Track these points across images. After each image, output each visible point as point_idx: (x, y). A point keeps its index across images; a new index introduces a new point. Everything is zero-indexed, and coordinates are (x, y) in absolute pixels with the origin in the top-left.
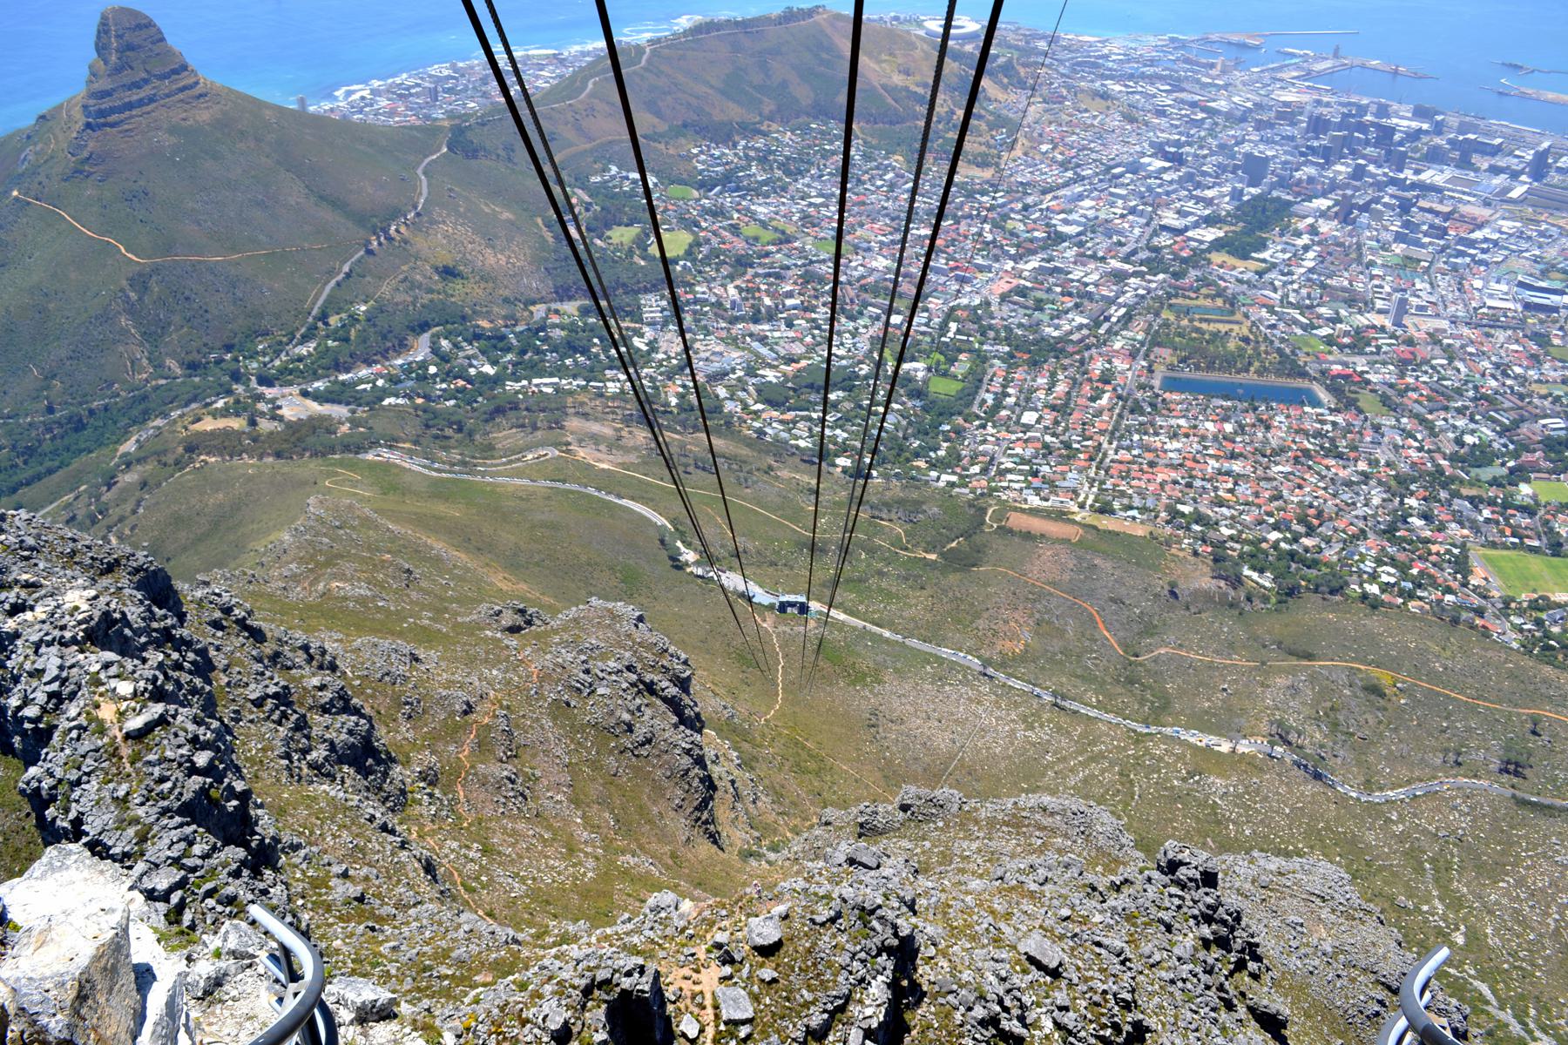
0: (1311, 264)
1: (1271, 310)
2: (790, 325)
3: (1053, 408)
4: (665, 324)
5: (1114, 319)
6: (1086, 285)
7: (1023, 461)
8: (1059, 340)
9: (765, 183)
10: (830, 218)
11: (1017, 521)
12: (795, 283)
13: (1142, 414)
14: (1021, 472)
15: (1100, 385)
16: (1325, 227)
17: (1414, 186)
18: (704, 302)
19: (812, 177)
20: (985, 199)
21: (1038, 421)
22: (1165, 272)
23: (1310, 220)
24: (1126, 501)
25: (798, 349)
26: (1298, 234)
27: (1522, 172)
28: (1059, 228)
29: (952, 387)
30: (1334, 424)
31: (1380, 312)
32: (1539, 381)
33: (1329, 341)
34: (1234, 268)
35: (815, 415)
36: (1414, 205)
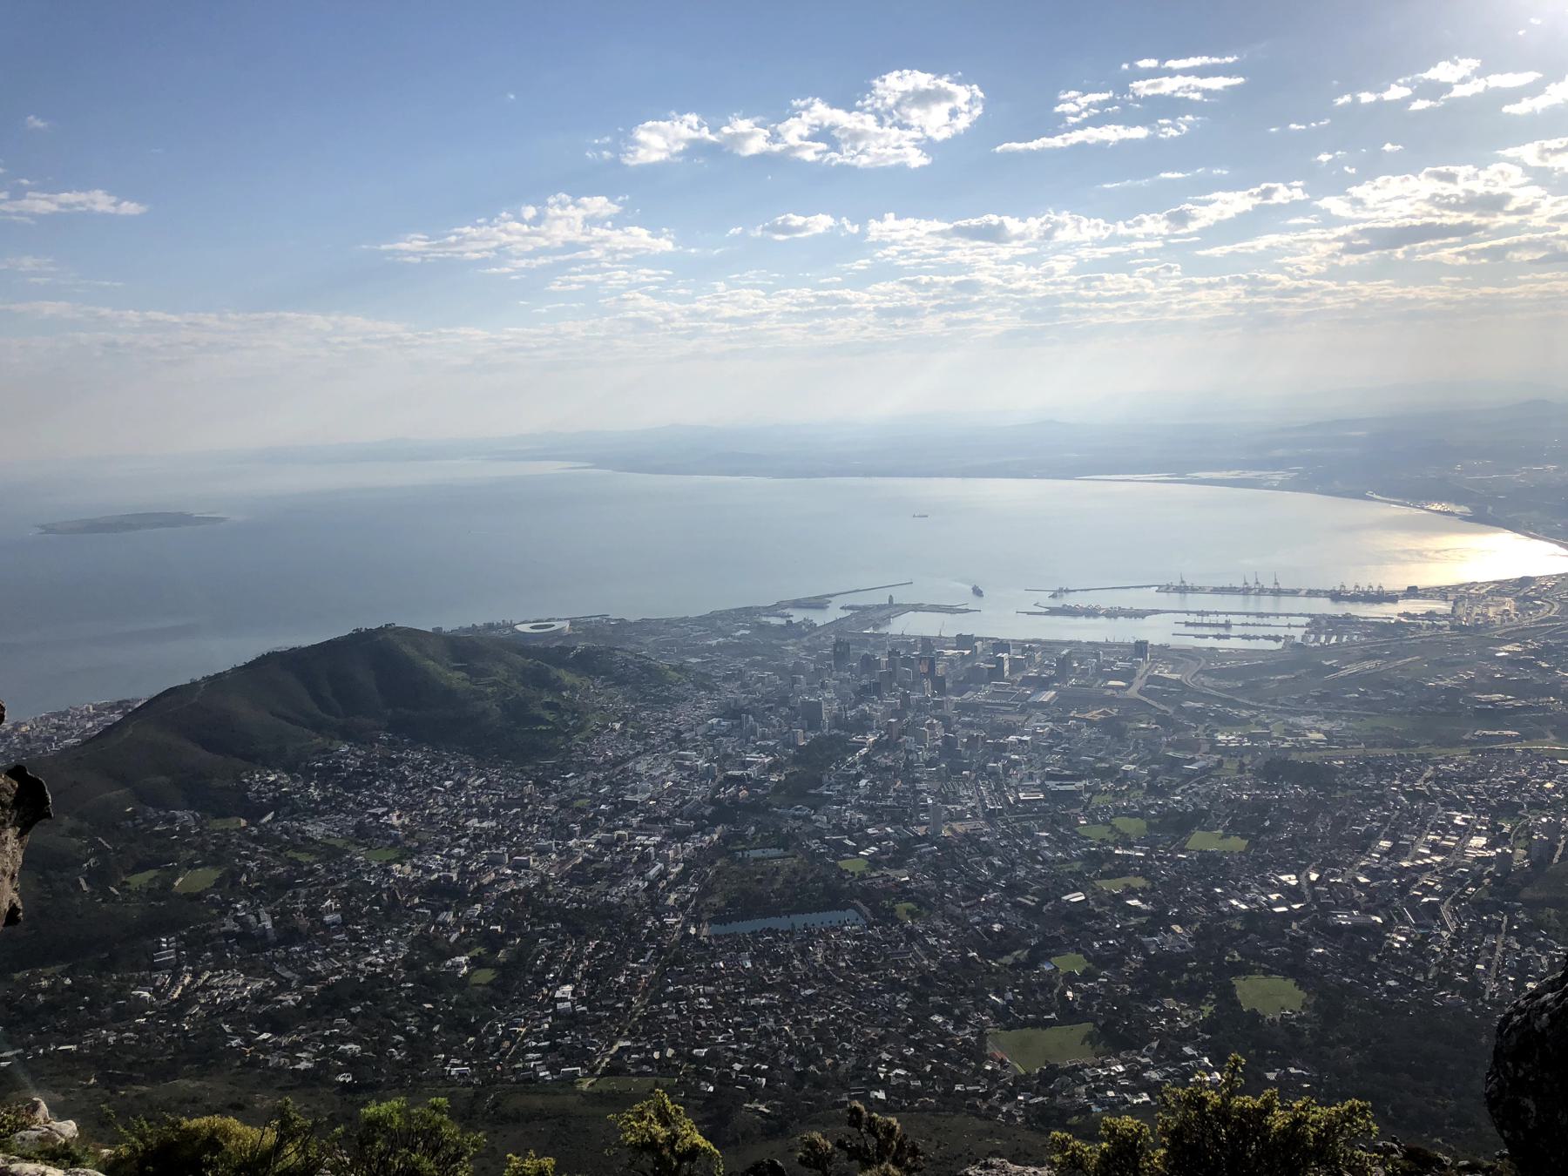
18: (228, 935)
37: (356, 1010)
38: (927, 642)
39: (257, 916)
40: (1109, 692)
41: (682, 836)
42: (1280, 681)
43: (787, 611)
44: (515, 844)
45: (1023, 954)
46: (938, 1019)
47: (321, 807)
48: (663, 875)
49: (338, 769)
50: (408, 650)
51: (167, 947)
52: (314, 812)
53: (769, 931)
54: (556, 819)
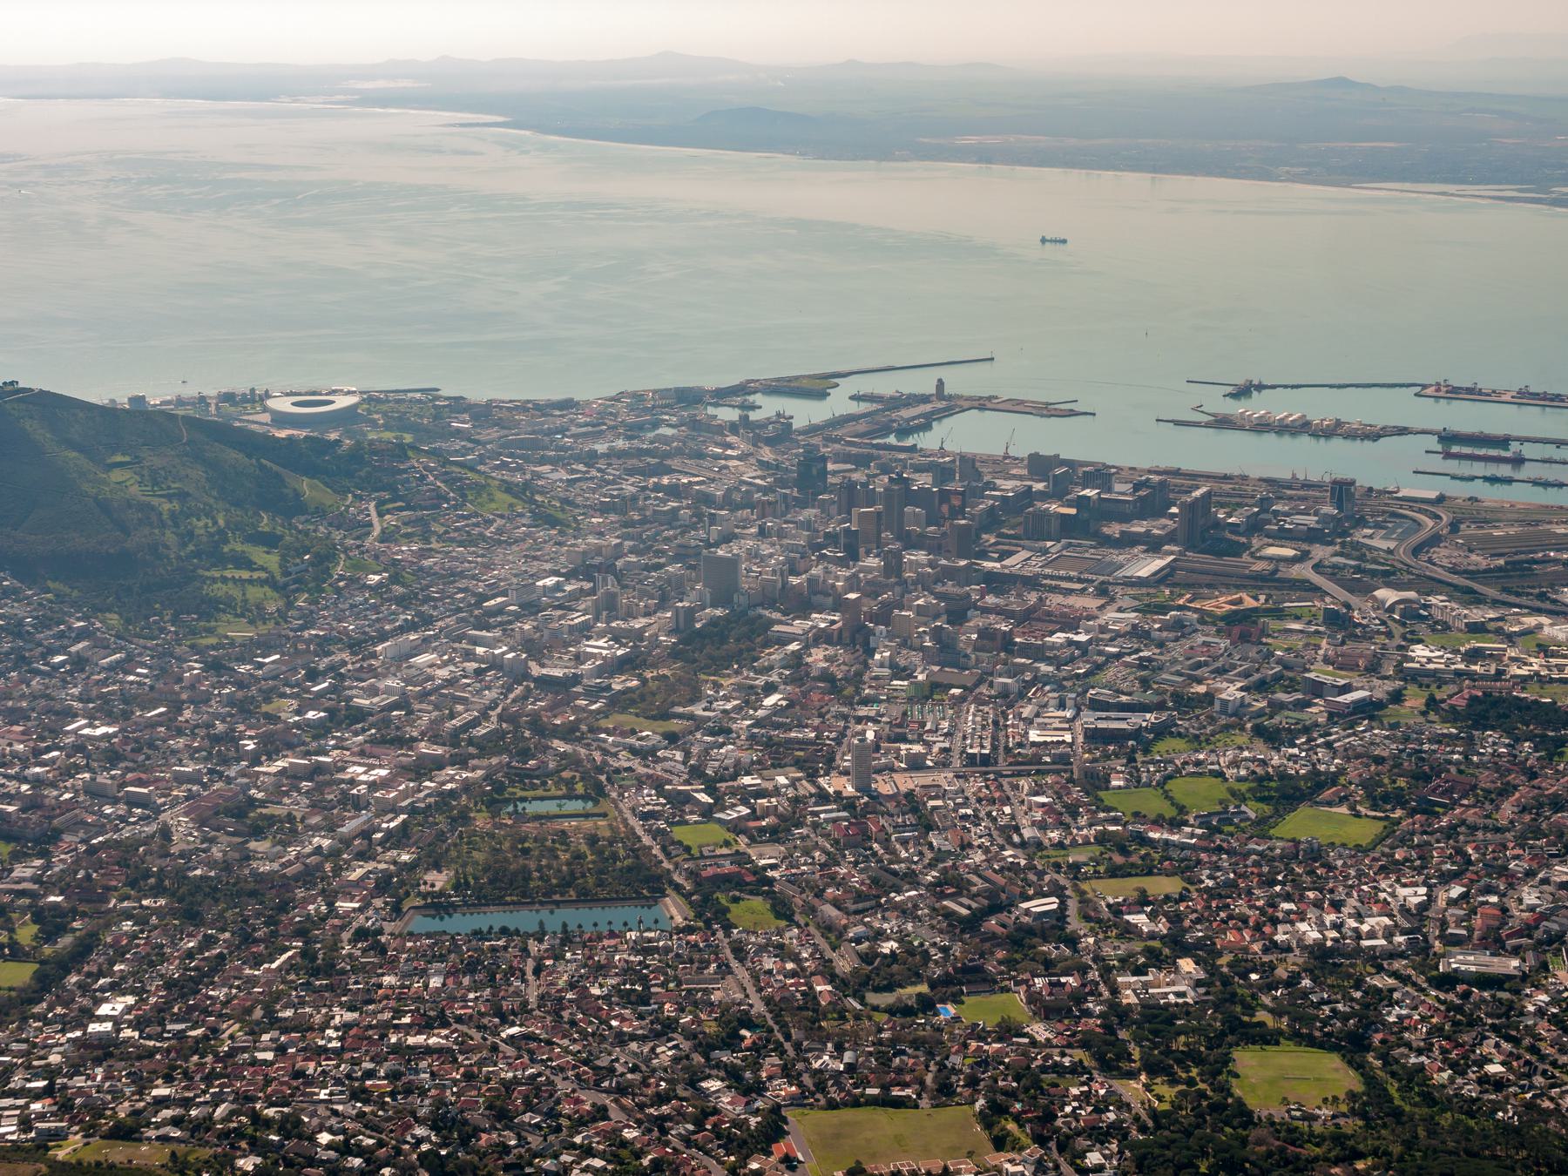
0: (760, 713)
7: (50, 1073)
8: (260, 878)
16: (817, 657)
23: (794, 647)
27: (1171, 538)
32: (1060, 845)
33: (736, 827)
34: (633, 732)
38: (969, 464)
40: (1259, 566)
45: (910, 992)
48: (366, 834)
53: (504, 931)
54: (220, 727)
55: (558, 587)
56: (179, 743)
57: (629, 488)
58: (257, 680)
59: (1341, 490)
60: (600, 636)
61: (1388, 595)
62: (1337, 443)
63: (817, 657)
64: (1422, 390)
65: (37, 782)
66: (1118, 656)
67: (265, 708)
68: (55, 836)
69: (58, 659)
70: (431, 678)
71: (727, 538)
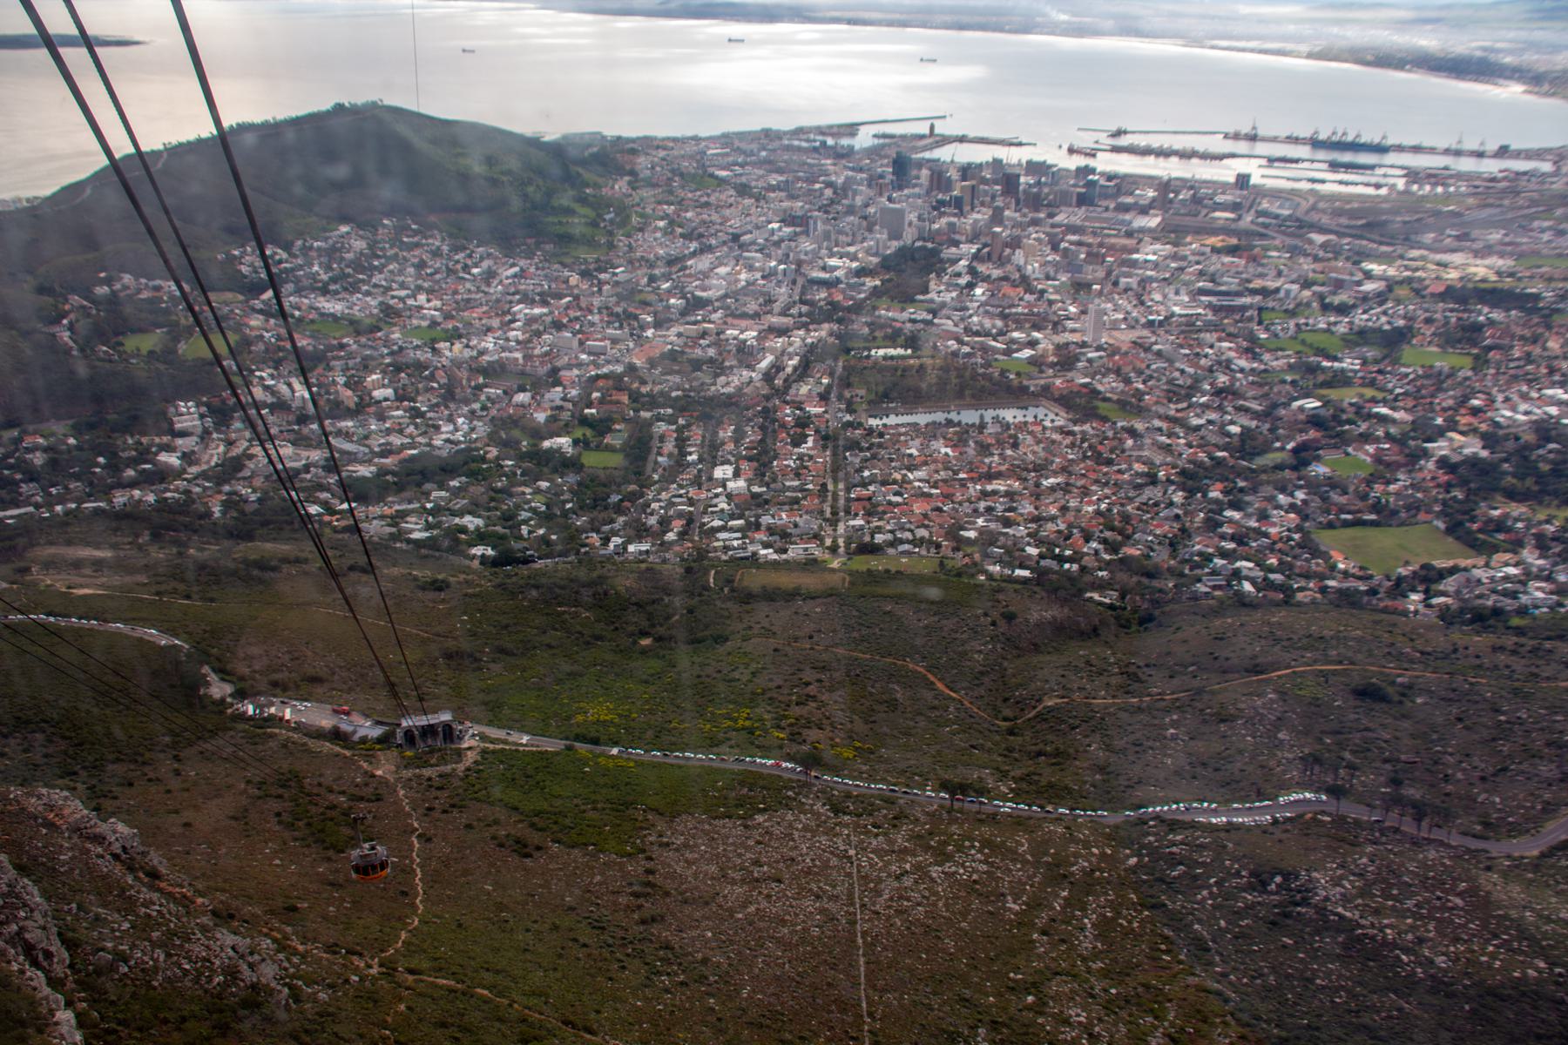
1: (960, 342)
2: (382, 418)
3: (750, 459)
4: (205, 435)
5: (789, 370)
6: (745, 341)
8: (729, 396)
9: (334, 280)
10: (422, 308)
11: (754, 580)
12: (384, 372)
13: (861, 450)
14: (732, 530)
15: (799, 430)
16: (981, 268)
17: (1053, 226)
19: (391, 272)
20: (603, 276)
21: (737, 474)
22: (829, 319)
24: (889, 537)
25: (397, 440)
26: (959, 275)
28: (699, 293)
29: (616, 460)
30: (1083, 432)
31: (1073, 331)
33: (1032, 361)
34: (903, 310)
35: (429, 506)
36: (1062, 240)
37: (454, 483)
39: (289, 385)
41: (782, 332)
42: (1405, 223)
43: (812, 136)
44: (579, 332)
46: (1236, 515)
47: (332, 287)
48: (777, 367)
49: (339, 250)
50: (403, 129)
51: (188, 415)
52: (325, 291)
54: (619, 310)
55: (780, 229)
56: (596, 318)
57: (774, 179)
58: (617, 283)
59: (1243, 180)
60: (832, 255)
61: (1319, 238)
62: (1195, 161)
63: (981, 268)
64: (1226, 136)
65: (518, 342)
66: (1182, 269)
67: (638, 298)
68: (555, 371)
69: (475, 271)
70: (738, 280)
71: (867, 205)
